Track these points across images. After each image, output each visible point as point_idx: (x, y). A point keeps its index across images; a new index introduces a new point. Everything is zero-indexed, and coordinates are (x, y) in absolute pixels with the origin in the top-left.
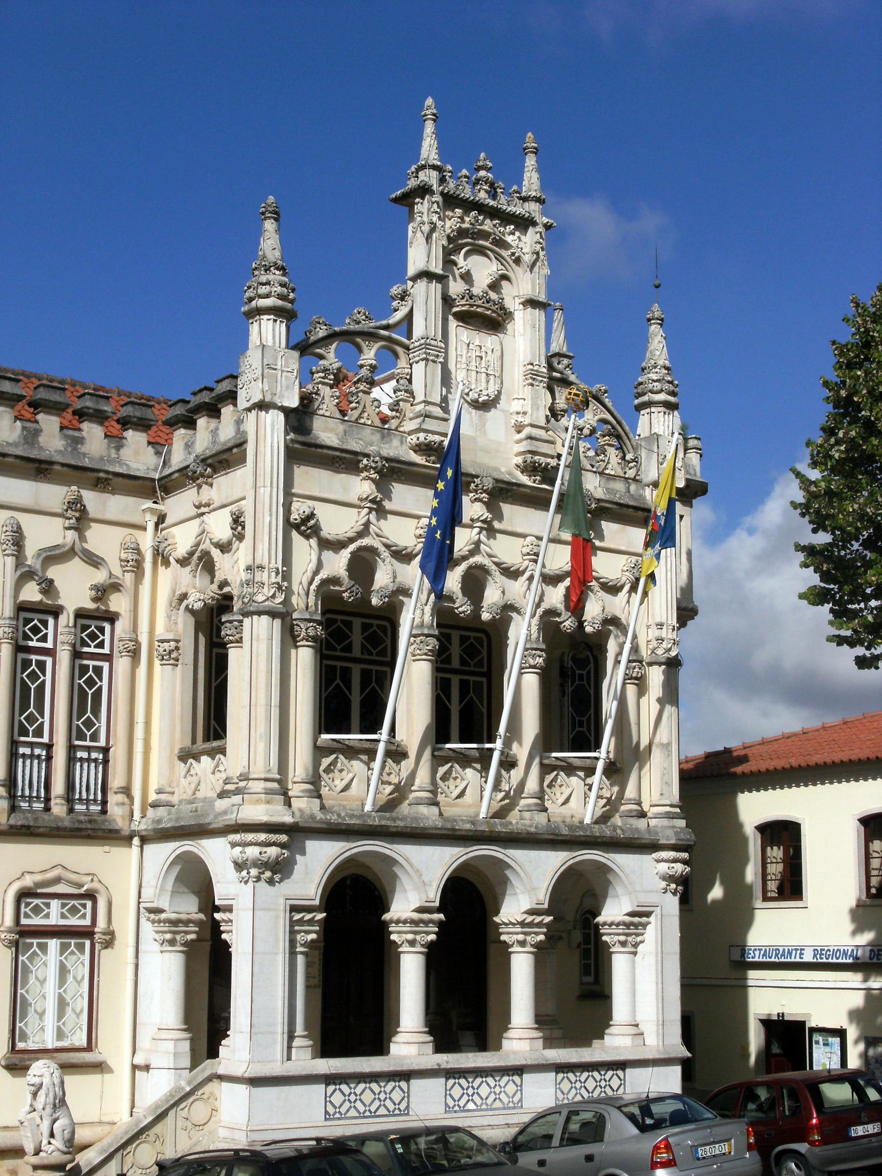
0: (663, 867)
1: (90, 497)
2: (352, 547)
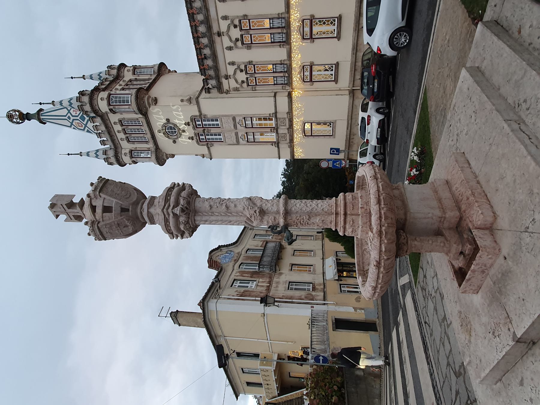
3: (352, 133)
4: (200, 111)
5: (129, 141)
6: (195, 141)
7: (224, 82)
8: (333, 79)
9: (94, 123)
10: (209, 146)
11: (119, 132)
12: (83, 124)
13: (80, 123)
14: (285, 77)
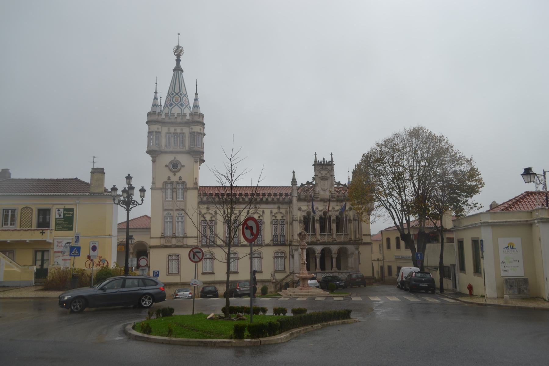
0: (355, 247)
1: (281, 206)
2: (306, 211)
4: (189, 189)
5: (167, 133)
7: (205, 206)
8: (204, 271)
10: (163, 190)
11: (175, 130)
12: (178, 103)
13: (178, 101)
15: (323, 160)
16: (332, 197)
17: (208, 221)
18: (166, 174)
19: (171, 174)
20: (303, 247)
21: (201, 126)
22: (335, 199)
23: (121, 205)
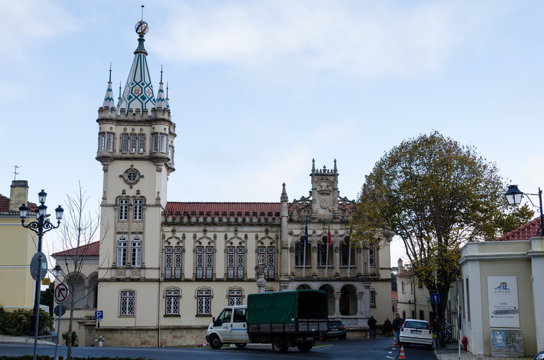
0: (365, 284)
1: (269, 228)
3: (123, 331)
4: (150, 206)
5: (123, 134)
6: (121, 195)
7: (170, 229)
9: (143, 112)
10: (116, 207)
14: (171, 276)
15: (323, 169)
16: (335, 218)
17: (174, 248)
18: (119, 187)
19: (126, 187)
20: (261, 284)
21: (167, 126)
22: (338, 221)
23: (32, 228)
